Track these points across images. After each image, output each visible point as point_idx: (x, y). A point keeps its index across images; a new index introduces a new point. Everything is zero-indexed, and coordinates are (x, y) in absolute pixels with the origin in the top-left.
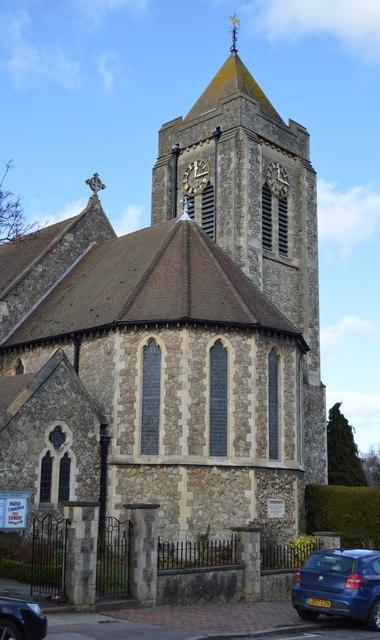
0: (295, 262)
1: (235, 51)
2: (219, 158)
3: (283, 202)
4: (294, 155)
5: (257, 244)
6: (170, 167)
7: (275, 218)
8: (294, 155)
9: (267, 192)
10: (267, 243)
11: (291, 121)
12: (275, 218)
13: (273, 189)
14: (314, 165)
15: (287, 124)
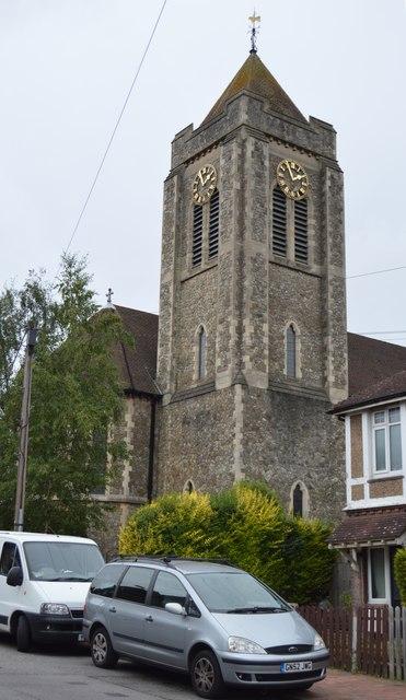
0: (315, 269)
1: (253, 51)
2: (222, 162)
3: (301, 205)
4: (315, 154)
5: (265, 250)
6: (181, 178)
7: (291, 227)
8: (315, 154)
9: (279, 194)
10: (279, 245)
11: (311, 118)
12: (291, 227)
13: (287, 190)
14: (341, 165)
15: (308, 119)
